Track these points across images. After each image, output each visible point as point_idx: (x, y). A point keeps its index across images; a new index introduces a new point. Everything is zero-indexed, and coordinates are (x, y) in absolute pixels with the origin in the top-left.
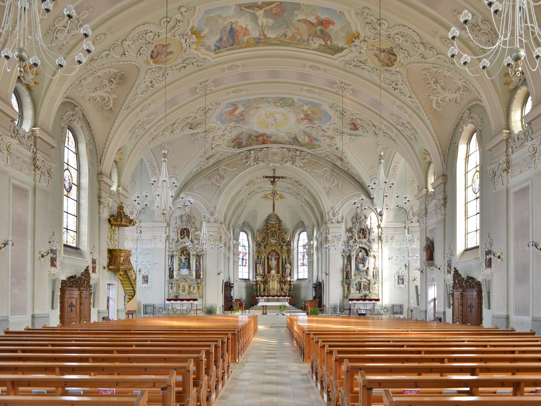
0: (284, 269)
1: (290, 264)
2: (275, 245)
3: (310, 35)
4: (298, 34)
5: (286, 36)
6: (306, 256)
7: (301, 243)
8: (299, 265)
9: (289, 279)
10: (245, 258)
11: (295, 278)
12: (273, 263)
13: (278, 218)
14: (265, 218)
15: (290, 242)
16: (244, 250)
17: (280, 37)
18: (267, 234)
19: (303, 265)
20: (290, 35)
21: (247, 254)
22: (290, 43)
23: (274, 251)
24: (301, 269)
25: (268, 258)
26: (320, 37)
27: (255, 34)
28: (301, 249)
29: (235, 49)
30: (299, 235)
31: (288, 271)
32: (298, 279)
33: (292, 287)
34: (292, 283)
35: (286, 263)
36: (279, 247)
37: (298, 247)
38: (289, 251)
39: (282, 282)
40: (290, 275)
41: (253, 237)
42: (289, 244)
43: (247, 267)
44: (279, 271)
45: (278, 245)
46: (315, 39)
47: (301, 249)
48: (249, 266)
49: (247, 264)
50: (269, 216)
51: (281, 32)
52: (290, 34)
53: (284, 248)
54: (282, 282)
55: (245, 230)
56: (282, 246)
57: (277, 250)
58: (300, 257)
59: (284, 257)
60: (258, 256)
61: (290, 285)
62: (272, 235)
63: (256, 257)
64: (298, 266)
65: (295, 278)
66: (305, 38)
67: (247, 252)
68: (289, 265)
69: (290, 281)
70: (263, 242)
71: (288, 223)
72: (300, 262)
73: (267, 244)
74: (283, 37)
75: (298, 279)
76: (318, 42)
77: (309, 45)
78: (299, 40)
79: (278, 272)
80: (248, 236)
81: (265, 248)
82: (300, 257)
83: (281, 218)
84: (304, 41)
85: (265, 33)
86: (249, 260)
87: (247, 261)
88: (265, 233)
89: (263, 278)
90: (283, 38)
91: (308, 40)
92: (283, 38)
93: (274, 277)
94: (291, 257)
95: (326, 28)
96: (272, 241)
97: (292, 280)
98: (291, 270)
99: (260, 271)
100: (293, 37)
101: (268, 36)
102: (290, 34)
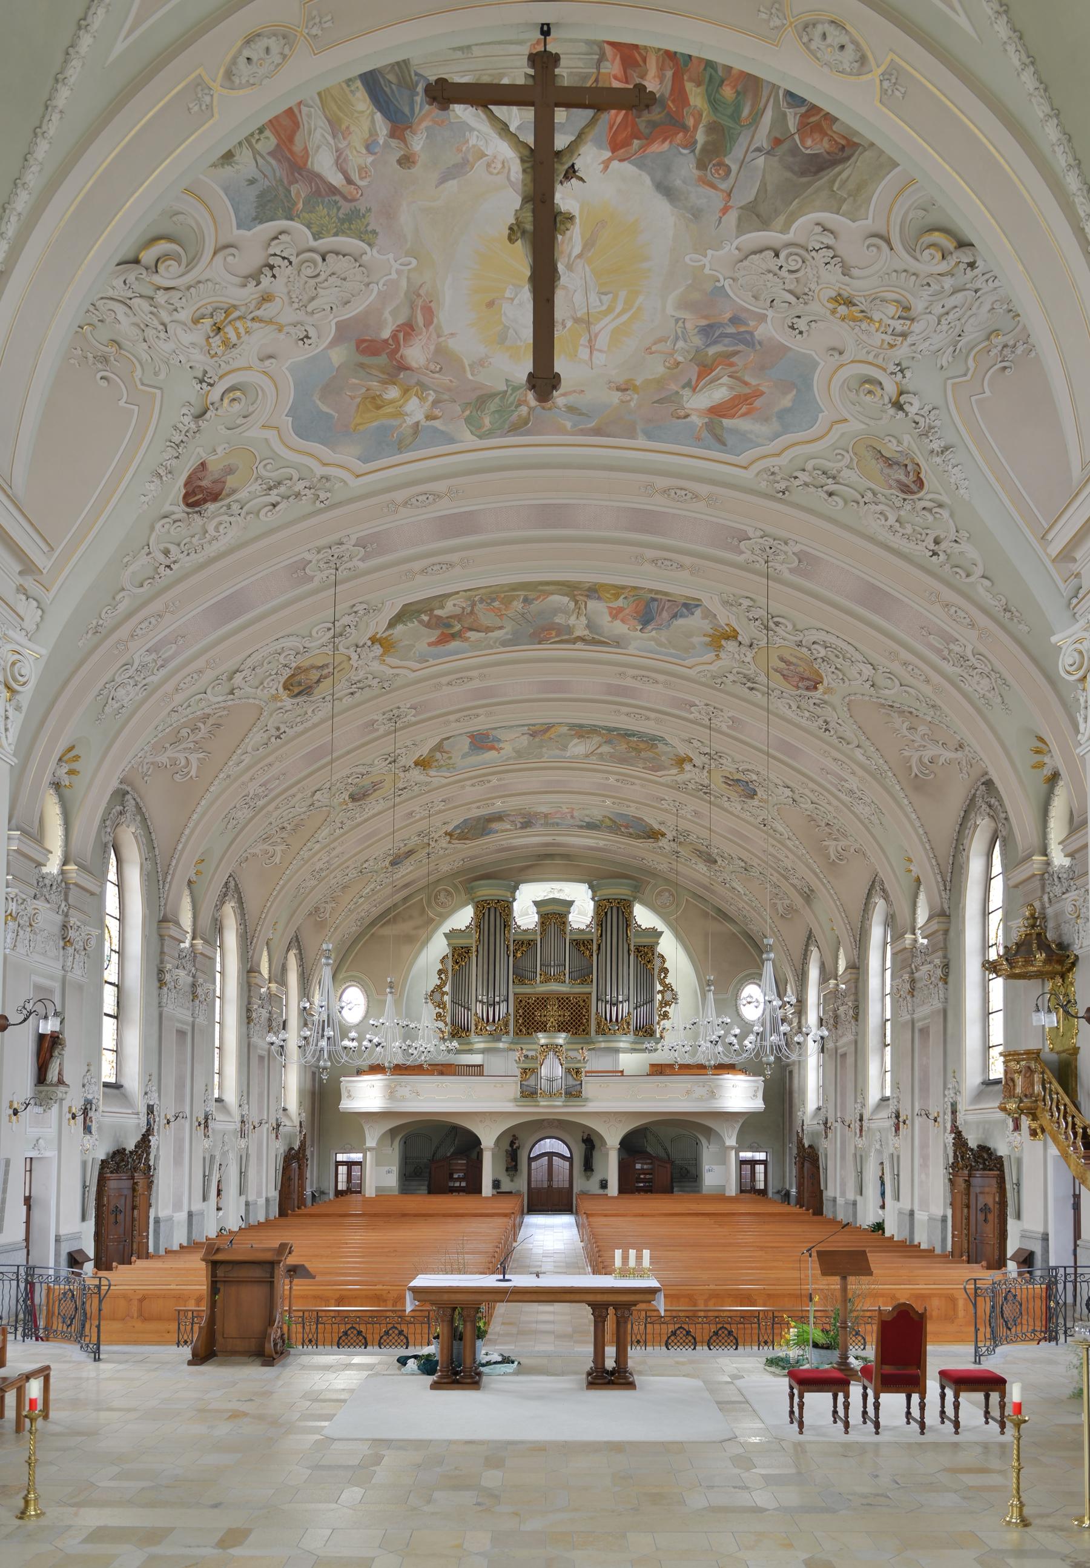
3: (472, 612)
4: (499, 609)
5: (526, 600)
17: (539, 597)
20: (515, 603)
22: (514, 590)
26: (450, 617)
27: (593, 605)
29: (651, 591)
46: (458, 611)
51: (535, 607)
52: (518, 605)
66: (479, 607)
74: (530, 597)
76: (450, 608)
77: (469, 599)
78: (493, 600)
84: (482, 601)
85: (572, 605)
90: (532, 595)
91: (473, 605)
92: (532, 595)
95: (443, 633)
100: (507, 602)
101: (566, 599)
102: (518, 605)
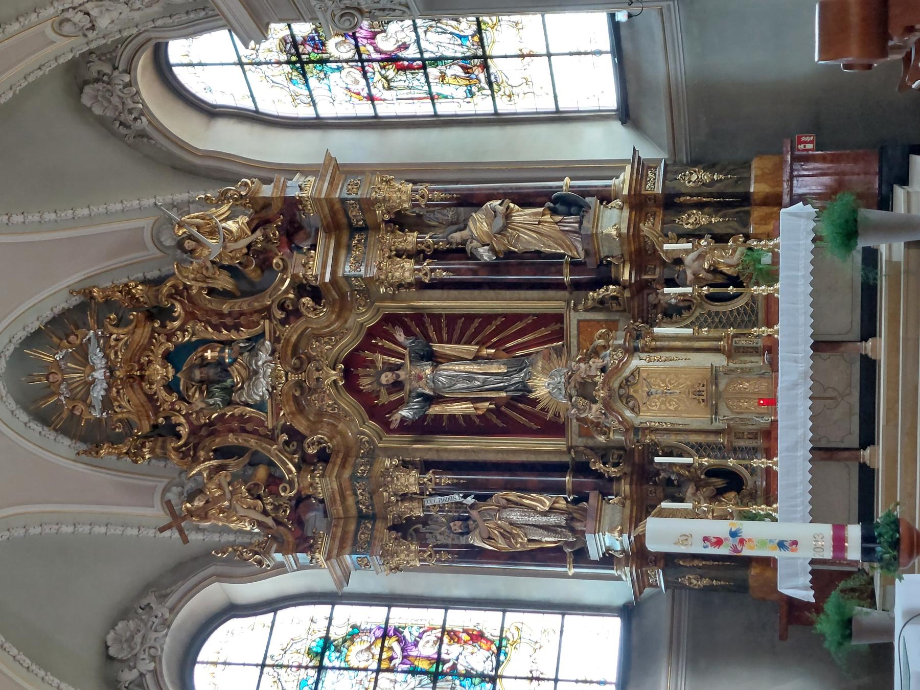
0: (517, 268)
1: (471, 202)
2: (297, 356)
6: (386, 43)
7: (276, 94)
8: (482, 105)
9: (612, 221)
10: (427, 649)
11: (610, 143)
12: (465, 375)
13: (62, 326)
14: (60, 452)
15: (261, 214)
16: (356, 654)
18: (202, 432)
19: (477, 63)
21: (401, 616)
23: (352, 366)
24: (525, 88)
25: (426, 427)
28: (337, 93)
30: (212, 112)
31: (533, 229)
32: (626, 114)
33: (694, 178)
34: (656, 186)
35: (459, 252)
36: (317, 317)
37: (318, 124)
38: (349, 223)
39: (633, 290)
40: (569, 205)
41: (244, 560)
42: (285, 223)
43: (513, 618)
44: (543, 320)
45: (292, 332)
47: (337, 93)
48: (504, 605)
49: (488, 621)
50: (44, 418)
53: (318, 263)
54: (641, 287)
55: (169, 644)
56: (302, 288)
57: (347, 344)
58: (401, 99)
59: (406, 270)
60: (404, 529)
61: (671, 203)
62: (206, 384)
63: (409, 552)
64: (498, 120)
65: (610, 143)
67: (372, 616)
68: (480, 224)
69: (639, 203)
70: (274, 480)
71: (107, 230)
72: (456, 101)
73: (295, 436)
75: (626, 114)
79: (551, 327)
80: (234, 610)
81: (324, 457)
82: (401, 99)
83: (51, 297)
86: (447, 603)
87: (459, 619)
88: (190, 454)
89: (606, 487)
93: (585, 390)
94: (401, 194)
96: (262, 389)
97: (622, 182)
98: (525, 200)
99: (534, 514)
